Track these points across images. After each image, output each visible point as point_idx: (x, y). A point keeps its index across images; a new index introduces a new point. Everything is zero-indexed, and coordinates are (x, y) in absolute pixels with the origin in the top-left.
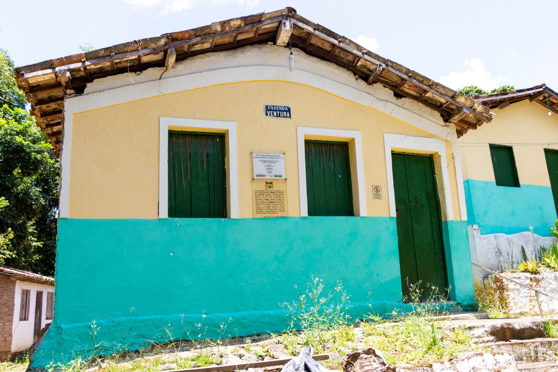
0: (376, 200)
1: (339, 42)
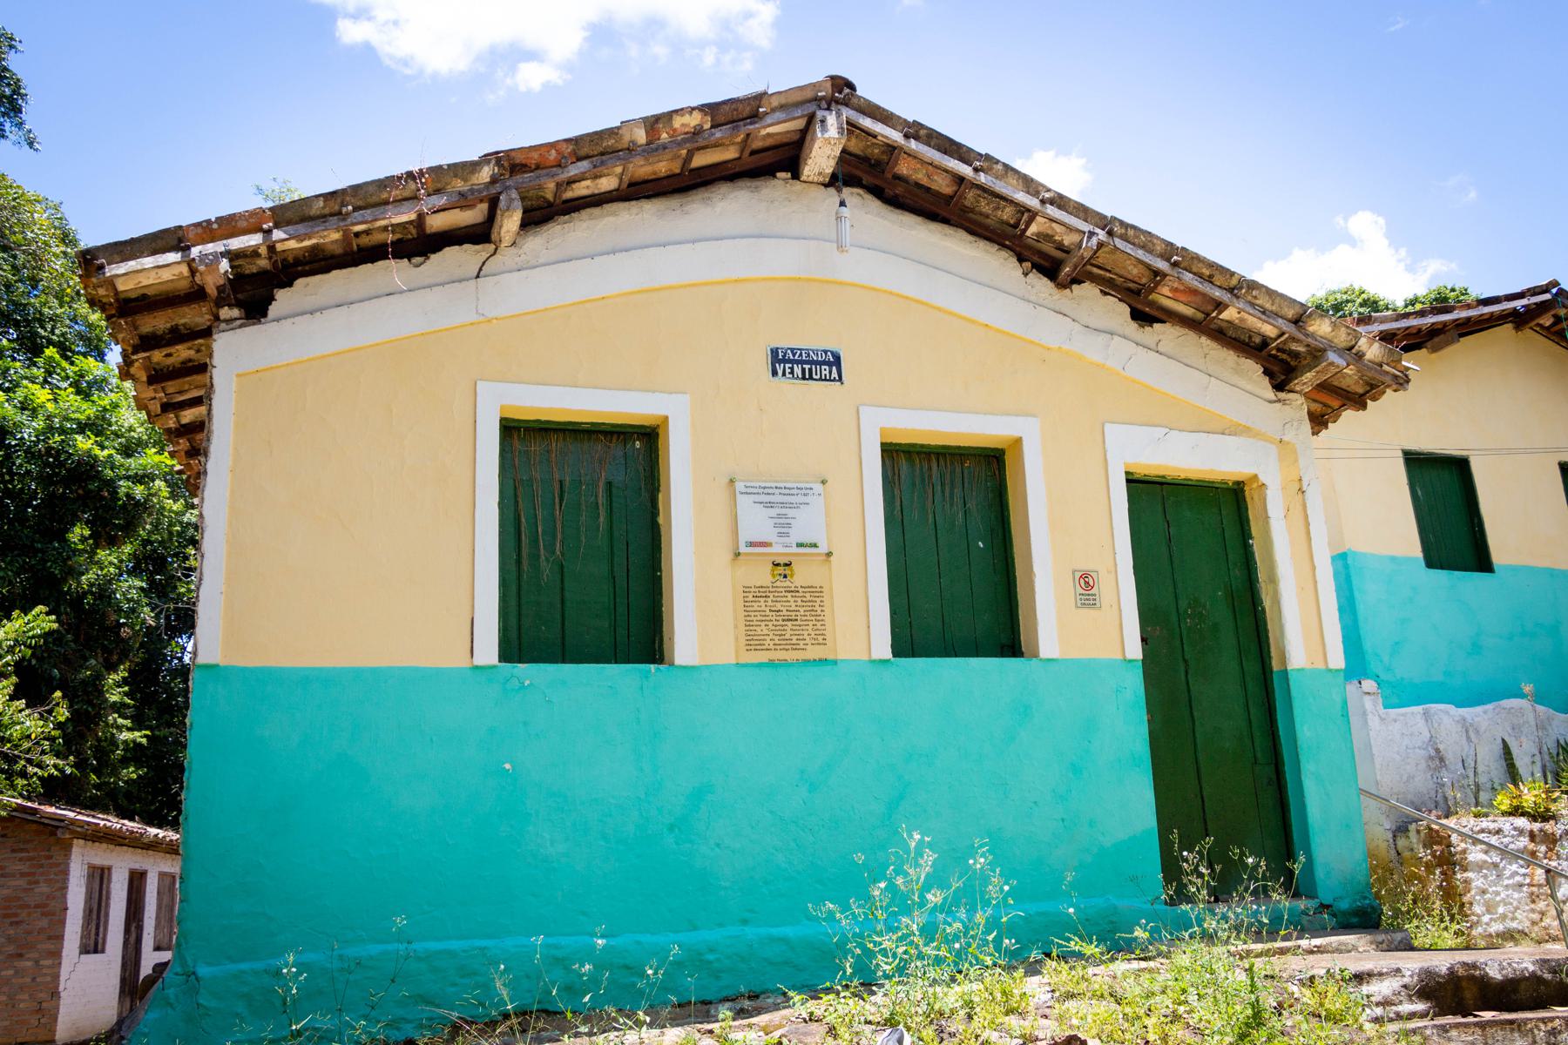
0: (1085, 611)
1: (976, 170)
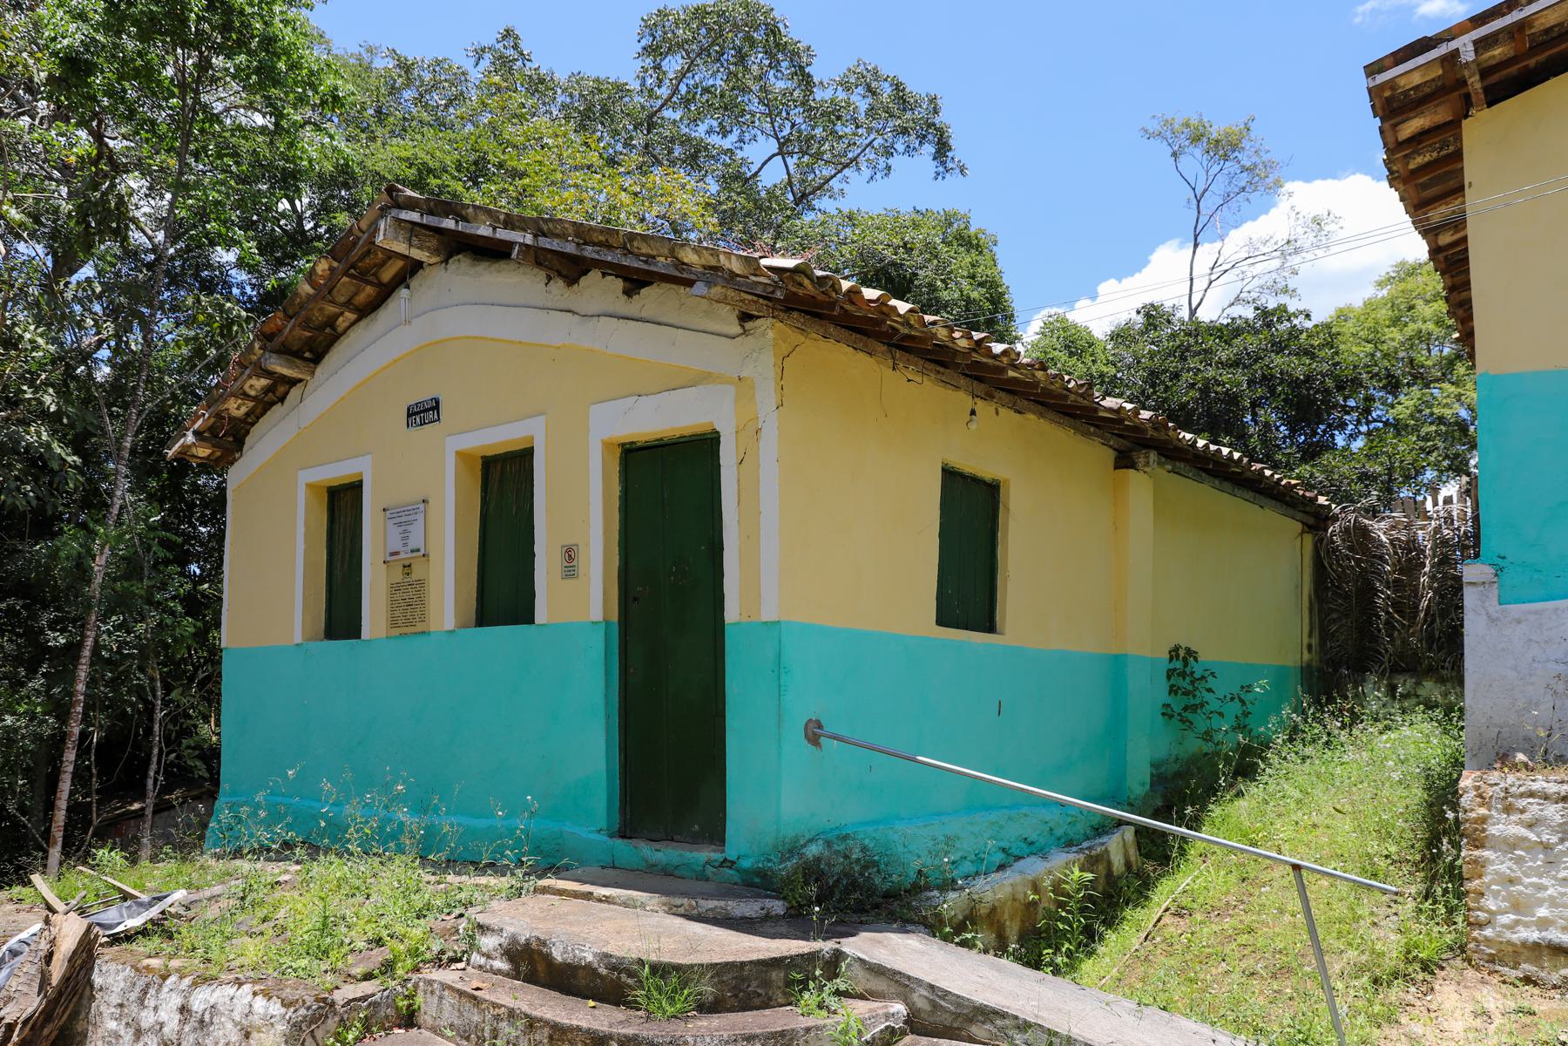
0: (568, 582)
